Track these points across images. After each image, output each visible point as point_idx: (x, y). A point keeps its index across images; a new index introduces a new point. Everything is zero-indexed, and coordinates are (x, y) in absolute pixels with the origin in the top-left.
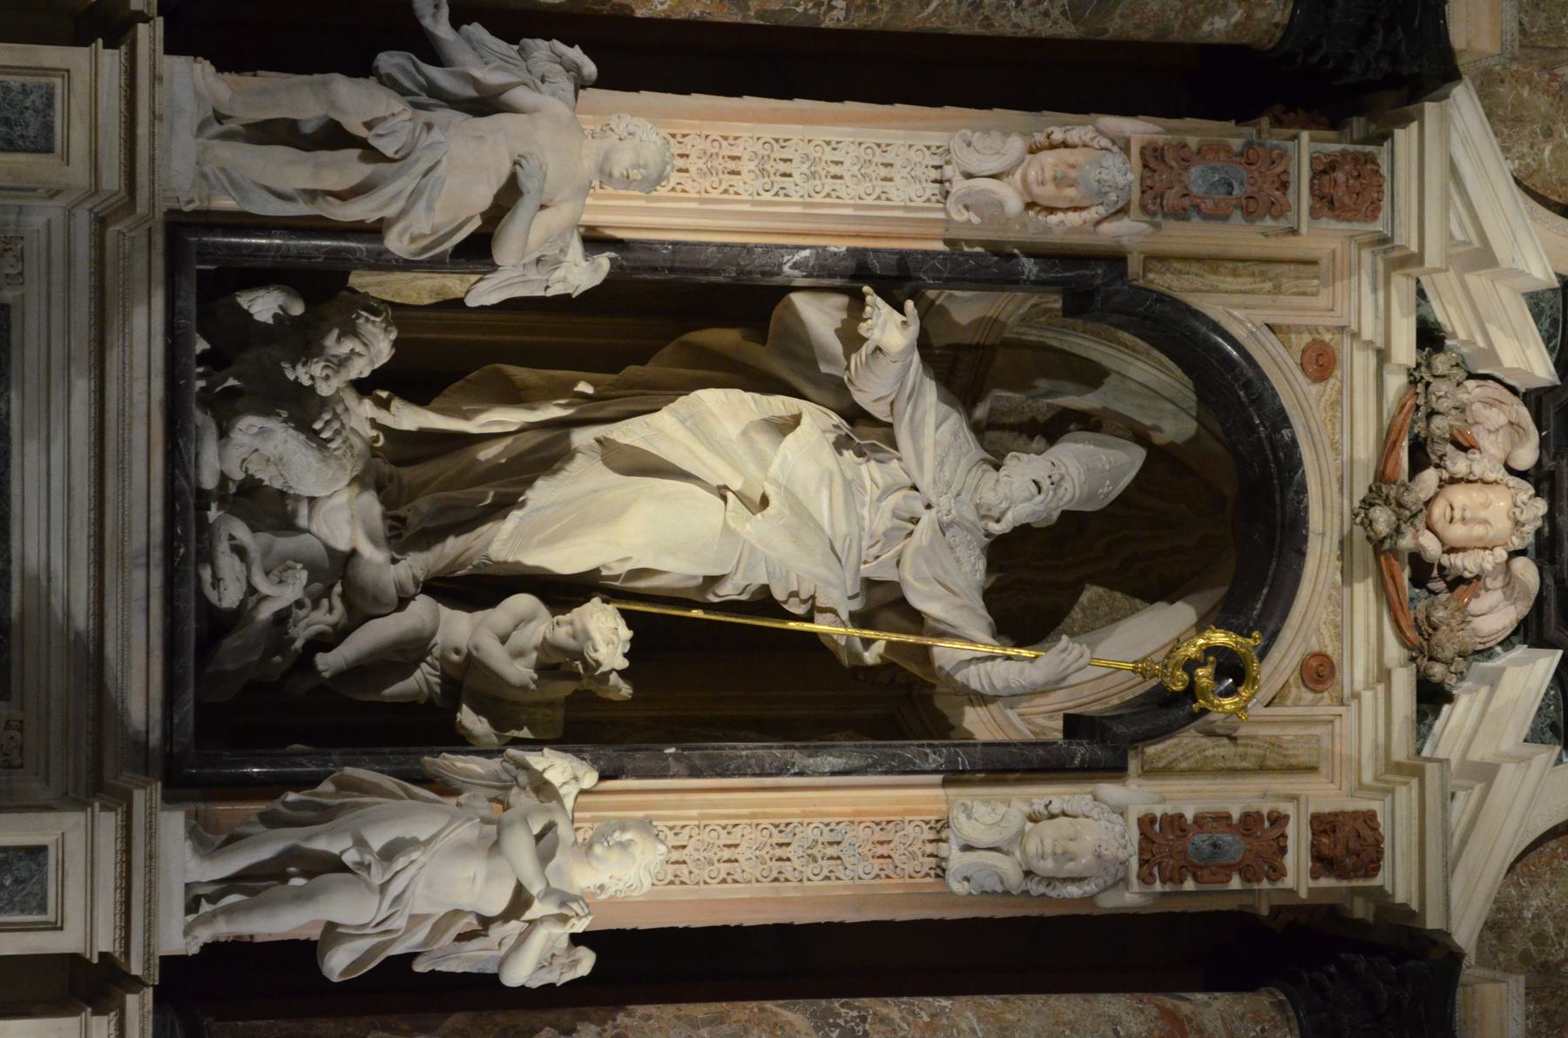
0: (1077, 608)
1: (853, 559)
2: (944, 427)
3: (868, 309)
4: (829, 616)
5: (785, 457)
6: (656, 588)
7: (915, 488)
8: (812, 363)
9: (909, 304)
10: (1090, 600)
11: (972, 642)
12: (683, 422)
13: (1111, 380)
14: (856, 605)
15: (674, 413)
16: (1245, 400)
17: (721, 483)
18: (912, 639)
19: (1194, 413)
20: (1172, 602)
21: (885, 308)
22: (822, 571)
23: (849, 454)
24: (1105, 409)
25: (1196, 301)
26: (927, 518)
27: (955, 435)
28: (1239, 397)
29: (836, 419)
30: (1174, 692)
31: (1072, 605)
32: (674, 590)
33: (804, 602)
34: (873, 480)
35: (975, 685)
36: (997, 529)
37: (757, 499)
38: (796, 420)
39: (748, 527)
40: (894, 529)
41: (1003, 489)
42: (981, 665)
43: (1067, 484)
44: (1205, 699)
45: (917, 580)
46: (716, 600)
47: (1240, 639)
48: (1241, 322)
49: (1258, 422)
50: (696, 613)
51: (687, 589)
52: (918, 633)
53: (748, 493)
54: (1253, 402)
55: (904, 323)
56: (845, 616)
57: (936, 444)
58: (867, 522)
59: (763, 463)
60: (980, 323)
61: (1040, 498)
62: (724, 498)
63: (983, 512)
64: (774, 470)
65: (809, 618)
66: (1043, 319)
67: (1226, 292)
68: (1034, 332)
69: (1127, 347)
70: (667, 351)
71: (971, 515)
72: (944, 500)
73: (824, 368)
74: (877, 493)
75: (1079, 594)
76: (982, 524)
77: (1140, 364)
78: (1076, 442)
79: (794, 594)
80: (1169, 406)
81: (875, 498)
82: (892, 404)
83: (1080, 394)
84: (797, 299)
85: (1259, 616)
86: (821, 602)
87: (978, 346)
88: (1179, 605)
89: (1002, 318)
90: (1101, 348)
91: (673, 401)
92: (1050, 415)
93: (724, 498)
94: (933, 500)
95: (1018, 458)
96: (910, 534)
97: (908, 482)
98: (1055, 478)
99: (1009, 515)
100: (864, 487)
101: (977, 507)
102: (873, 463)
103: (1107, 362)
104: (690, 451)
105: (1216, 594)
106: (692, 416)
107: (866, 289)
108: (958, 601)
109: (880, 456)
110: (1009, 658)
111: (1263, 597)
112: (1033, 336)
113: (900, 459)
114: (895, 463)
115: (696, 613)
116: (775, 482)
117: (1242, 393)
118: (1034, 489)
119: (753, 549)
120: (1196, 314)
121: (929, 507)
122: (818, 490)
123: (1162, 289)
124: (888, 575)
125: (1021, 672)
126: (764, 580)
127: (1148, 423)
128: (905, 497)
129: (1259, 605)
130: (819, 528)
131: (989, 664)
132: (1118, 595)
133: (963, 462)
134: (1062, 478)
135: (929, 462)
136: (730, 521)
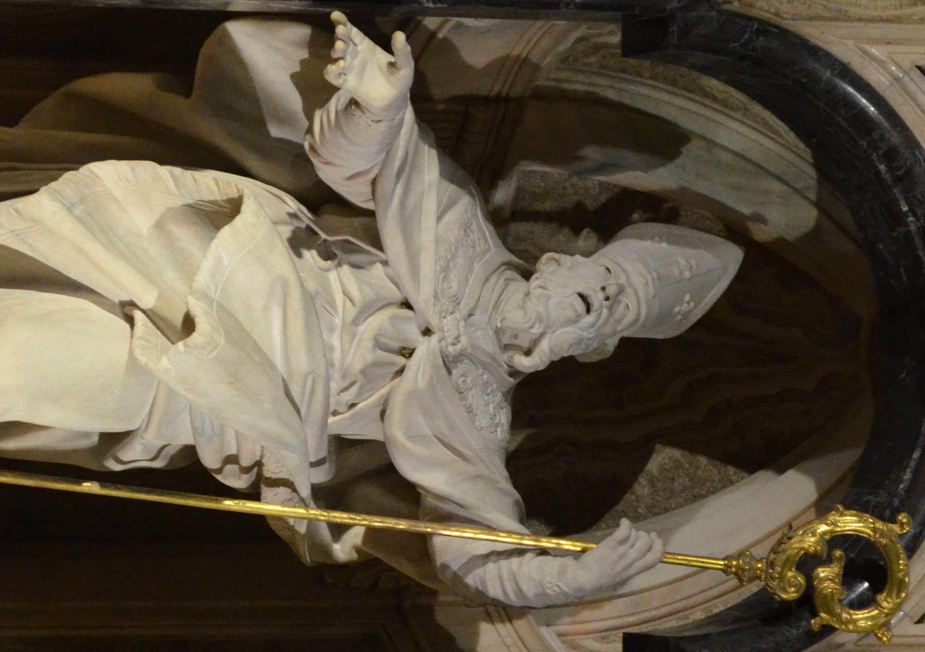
0: (642, 480)
1: (317, 408)
2: (450, 217)
3: (339, 45)
4: (283, 491)
5: (219, 261)
6: (30, 451)
7: (407, 305)
8: (259, 123)
9: (399, 38)
10: (662, 469)
11: (490, 528)
12: (70, 209)
13: (693, 148)
14: (321, 476)
15: (57, 196)
16: (887, 177)
17: (126, 298)
18: (402, 525)
19: (813, 197)
20: (781, 470)
21: (363, 43)
22: (273, 427)
23: (311, 256)
24: (684, 190)
25: (815, 33)
26: (425, 348)
27: (466, 228)
28: (878, 173)
29: (293, 205)
30: (784, 602)
31: (635, 475)
32: (56, 453)
33: (246, 470)
34: (346, 293)
35: (494, 591)
36: (526, 364)
37: (178, 320)
38: (234, 207)
39: (165, 362)
40: (377, 364)
41: (534, 307)
42: (504, 563)
43: (628, 300)
44: (830, 612)
45: (409, 438)
46: (118, 468)
47: (879, 525)
48: (881, 63)
49: (905, 209)
50: (90, 487)
51: (75, 452)
52: (412, 516)
53: (165, 313)
54: (898, 180)
55: (392, 65)
56: (305, 491)
57: (438, 241)
58: (337, 355)
59: (187, 269)
60: (501, 64)
61: (589, 319)
62: (130, 320)
63: (506, 340)
64: (202, 279)
65: (253, 494)
66: (593, 59)
67: (860, 20)
68: (581, 78)
69: (714, 99)
70: (47, 106)
71: (488, 345)
72: (449, 323)
73: (275, 131)
74: (352, 312)
75: (646, 459)
76: (505, 357)
77: (734, 125)
78: (642, 237)
79: (232, 459)
80: (777, 186)
81: (350, 317)
82: (374, 182)
83: (648, 168)
84: (236, 30)
85: (908, 490)
86: (270, 471)
87: (498, 99)
88: (792, 475)
89: (534, 58)
90: (678, 101)
91: (55, 179)
92: (603, 199)
93: (130, 320)
94: (434, 322)
95: (557, 261)
96: (401, 372)
97: (398, 296)
98: (611, 291)
99: (544, 345)
100: (332, 303)
101: (498, 332)
102: (346, 268)
103: (685, 122)
104: (82, 252)
105: (848, 457)
106: (83, 200)
107: (336, 15)
108: (469, 469)
109: (357, 258)
110: (543, 552)
111: (912, 464)
112: (579, 84)
113: (385, 263)
114: (378, 269)
115: (90, 487)
116: (204, 296)
117: (882, 167)
118: (580, 306)
119: (172, 394)
120: (816, 52)
121: (427, 332)
122: (266, 309)
123: (766, 15)
124: (370, 431)
125: (562, 573)
126: (188, 440)
127: (746, 210)
128: (393, 319)
129: (907, 476)
130: (267, 363)
131: (515, 561)
132: (703, 460)
133: (477, 267)
134: (621, 290)
135: (428, 267)
136: (138, 353)
